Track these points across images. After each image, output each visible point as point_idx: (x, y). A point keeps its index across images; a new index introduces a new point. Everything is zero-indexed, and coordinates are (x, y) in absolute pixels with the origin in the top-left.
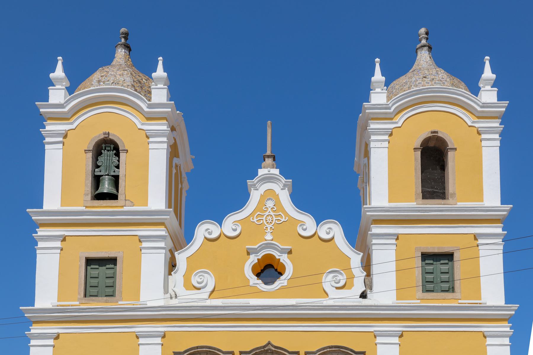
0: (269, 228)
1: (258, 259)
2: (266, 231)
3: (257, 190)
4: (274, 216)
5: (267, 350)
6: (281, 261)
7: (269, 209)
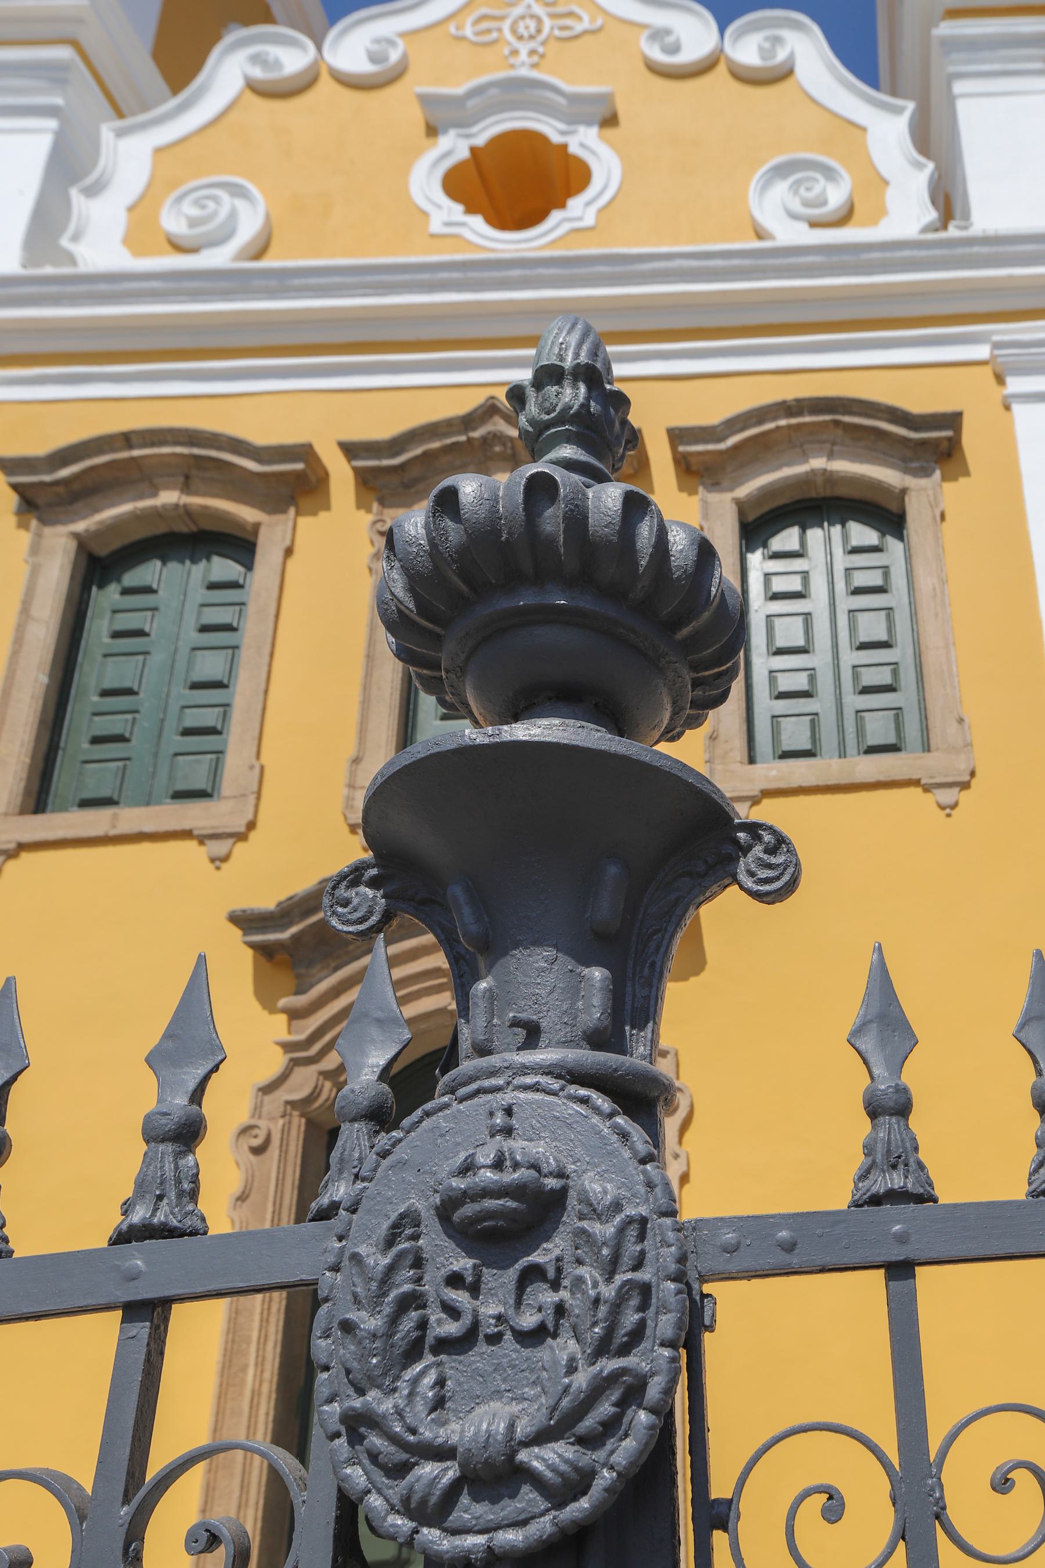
0: (523, 56)
1: (473, 150)
5: (486, 441)
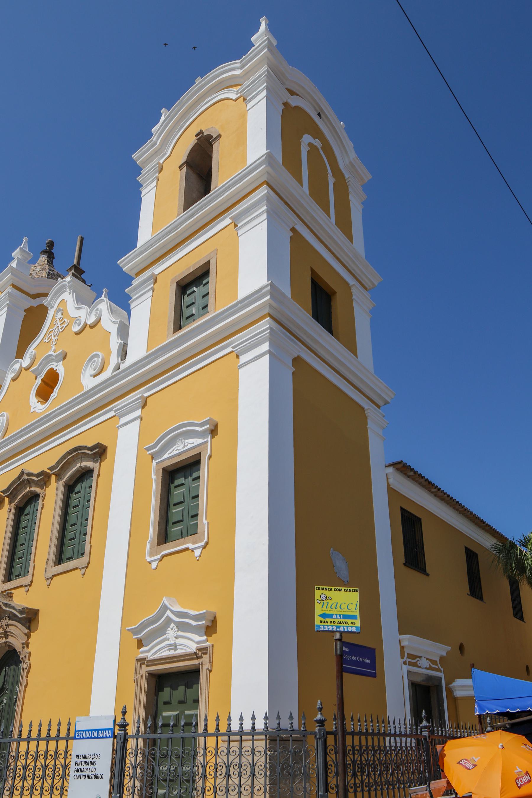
2: (52, 345)
3: (53, 307)
4: (59, 326)
6: (57, 371)
7: (58, 320)
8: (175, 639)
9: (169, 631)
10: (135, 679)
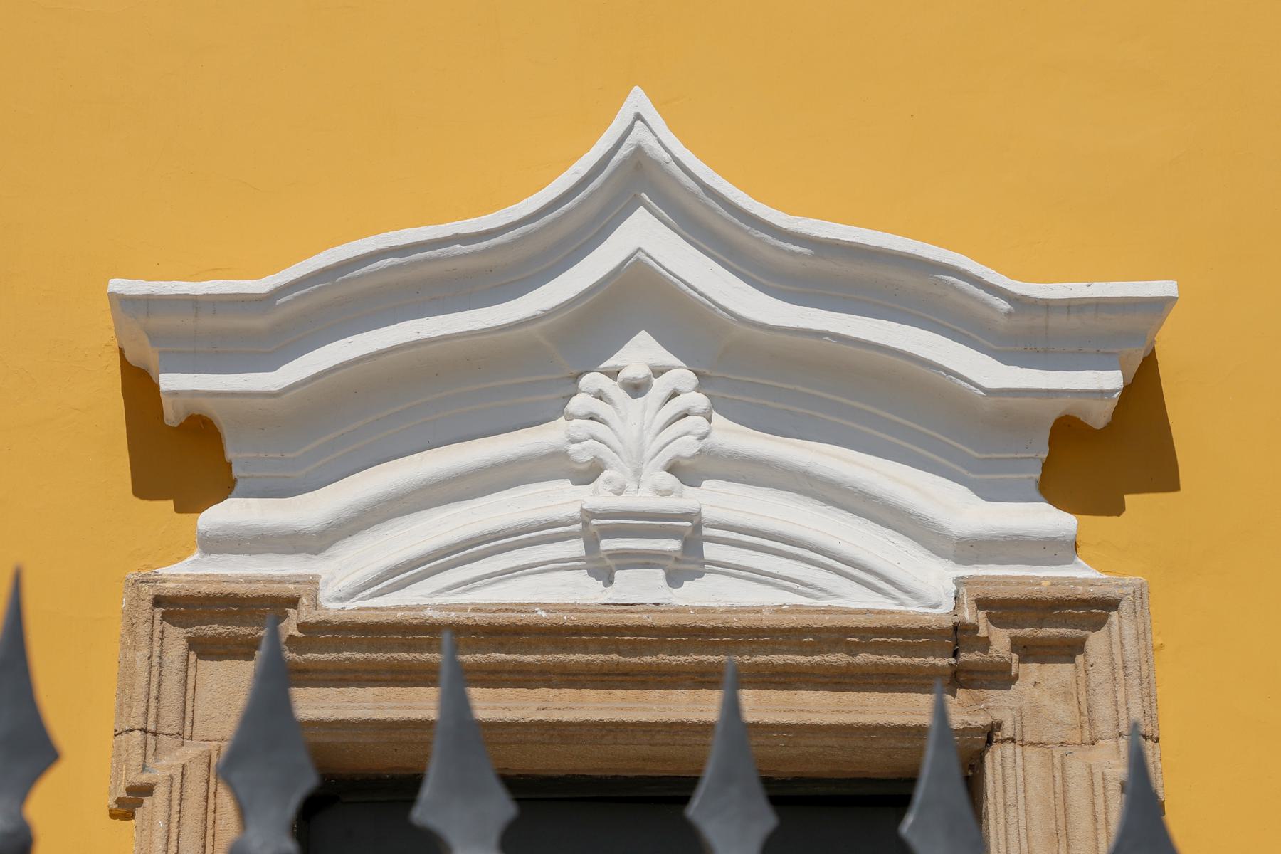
8: (670, 480)
9: (600, 396)
10: (158, 773)
